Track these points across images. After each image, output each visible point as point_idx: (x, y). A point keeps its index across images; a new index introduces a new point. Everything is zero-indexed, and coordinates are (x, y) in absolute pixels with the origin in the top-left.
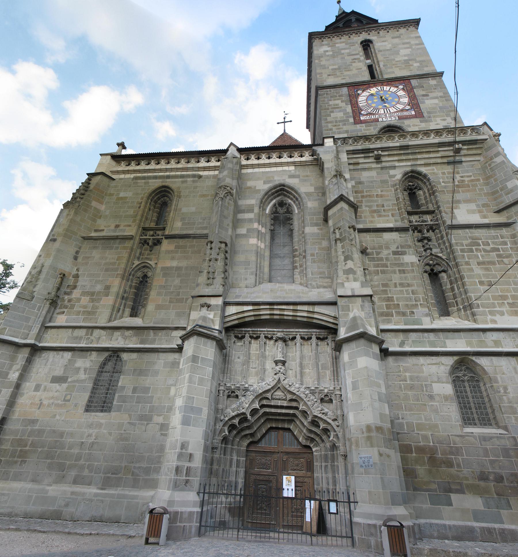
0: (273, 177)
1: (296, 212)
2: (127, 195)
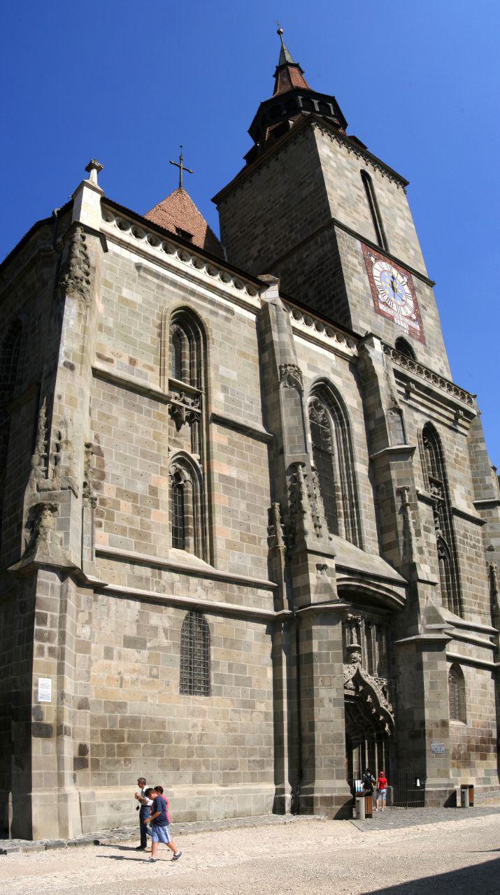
0: (316, 362)
1: (334, 428)
2: (135, 300)
